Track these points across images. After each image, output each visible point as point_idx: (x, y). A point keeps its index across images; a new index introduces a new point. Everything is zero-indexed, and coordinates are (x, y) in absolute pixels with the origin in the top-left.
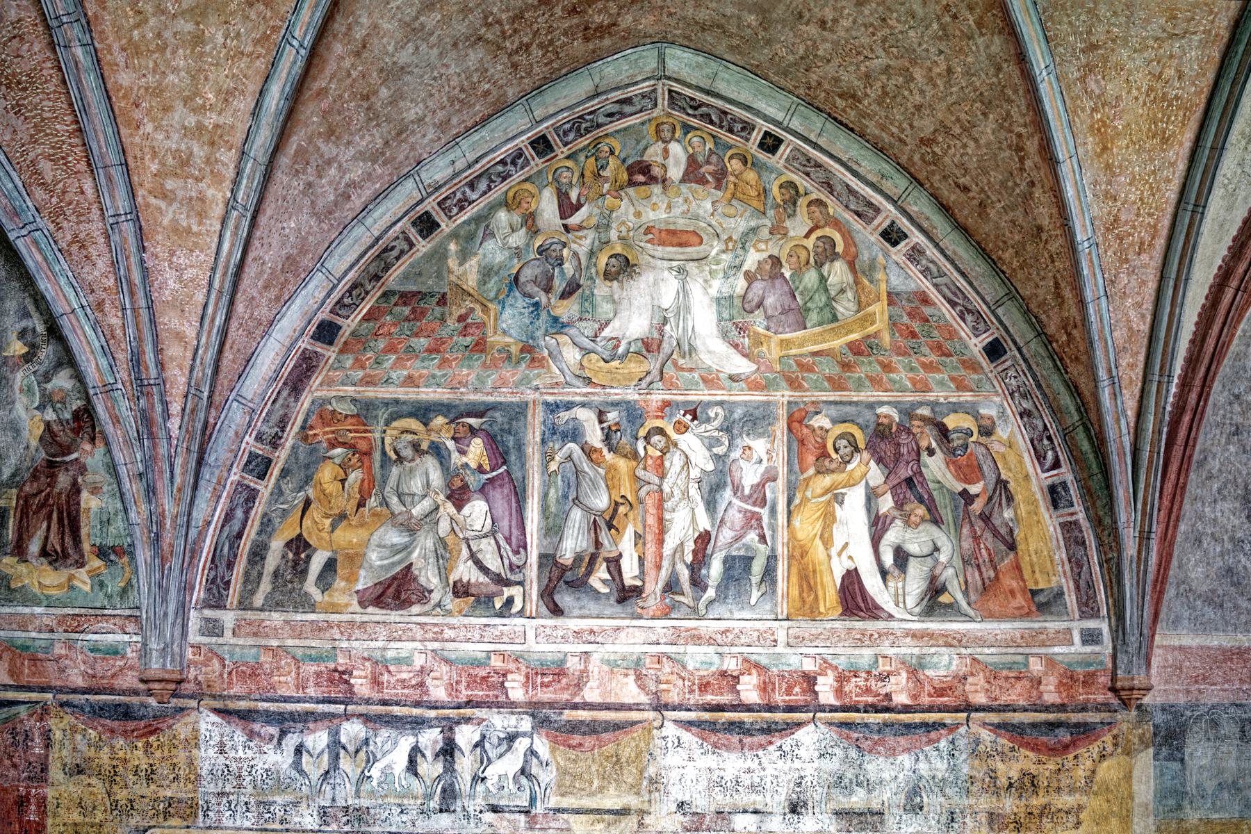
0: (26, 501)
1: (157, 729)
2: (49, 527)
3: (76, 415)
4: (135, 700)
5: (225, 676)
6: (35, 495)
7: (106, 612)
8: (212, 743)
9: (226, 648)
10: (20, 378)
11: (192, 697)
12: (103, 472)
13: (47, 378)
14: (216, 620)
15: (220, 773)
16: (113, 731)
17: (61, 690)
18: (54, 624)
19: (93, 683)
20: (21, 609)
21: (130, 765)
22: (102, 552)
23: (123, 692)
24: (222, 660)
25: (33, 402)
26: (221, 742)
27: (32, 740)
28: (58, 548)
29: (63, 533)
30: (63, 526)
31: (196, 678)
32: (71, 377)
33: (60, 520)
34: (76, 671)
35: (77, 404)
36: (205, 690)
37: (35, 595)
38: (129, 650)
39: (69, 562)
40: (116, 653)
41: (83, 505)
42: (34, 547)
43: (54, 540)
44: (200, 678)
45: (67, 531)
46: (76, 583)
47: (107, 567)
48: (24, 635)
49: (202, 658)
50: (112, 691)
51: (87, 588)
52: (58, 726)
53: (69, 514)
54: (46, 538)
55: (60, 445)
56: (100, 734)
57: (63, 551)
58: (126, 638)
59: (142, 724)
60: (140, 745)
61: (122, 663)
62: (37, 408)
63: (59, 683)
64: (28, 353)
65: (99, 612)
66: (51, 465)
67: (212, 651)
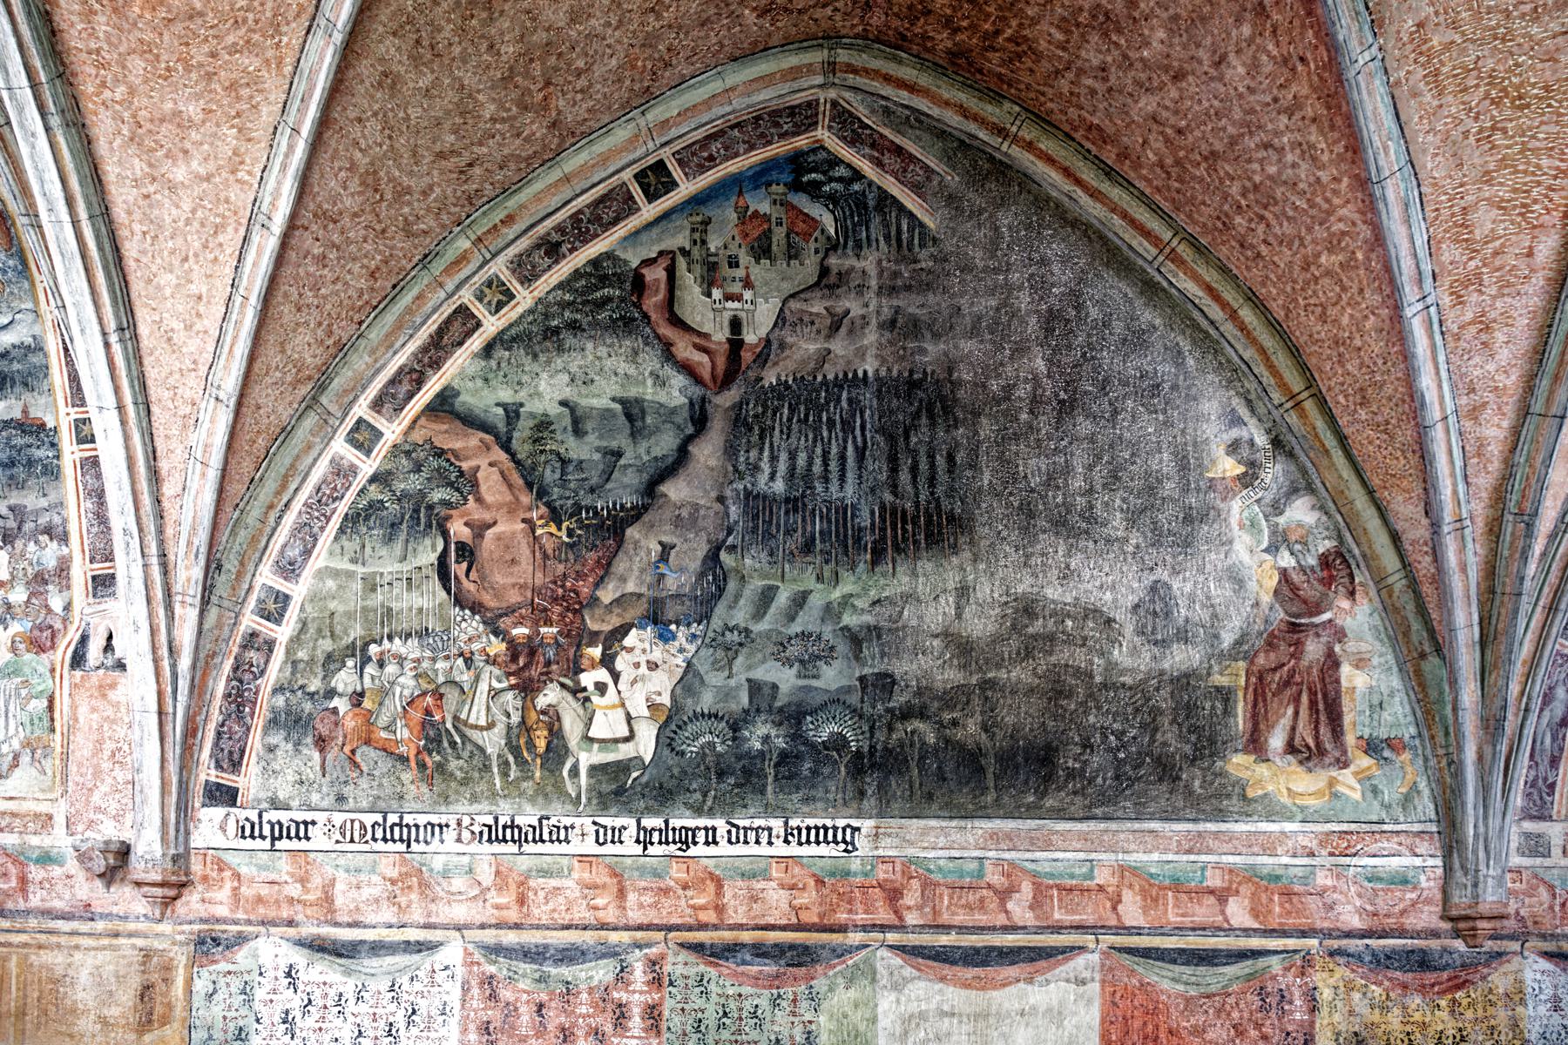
0: (1261, 678)
1: (1466, 981)
2: (1296, 713)
3: (1325, 561)
4: (1434, 944)
5: (1557, 908)
6: (1274, 670)
7: (1385, 827)
8: (1542, 997)
9: (1555, 871)
10: (1237, 508)
11: (1512, 937)
12: (1370, 639)
13: (1277, 508)
14: (1539, 836)
15: (1555, 1036)
16: (1405, 987)
17: (1328, 934)
18: (1314, 845)
19: (1374, 923)
20: (1264, 826)
21: (1431, 1031)
22: (1371, 747)
23: (1417, 935)
24: (1551, 888)
25: (1259, 542)
26: (1555, 996)
27: (1291, 1003)
28: (1312, 744)
29: (1317, 723)
30: (1317, 711)
31: (1517, 913)
32: (1313, 507)
33: (1313, 704)
34: (1349, 908)
35: (1325, 545)
36: (1531, 928)
37: (1285, 807)
38: (1423, 878)
39: (1327, 760)
40: (1405, 882)
41: (1344, 683)
42: (1277, 741)
43: (1305, 733)
44: (1522, 913)
45: (1323, 718)
46: (1340, 788)
47: (1380, 767)
48: (1270, 860)
49: (1524, 886)
50: (1402, 933)
51: (1357, 796)
52: (1326, 983)
53: (1325, 696)
54: (1293, 729)
55: (1305, 602)
56: (1387, 991)
57: (1318, 744)
58: (1418, 862)
59: (1445, 975)
60: (1443, 1003)
61: (1414, 896)
62: (1266, 551)
63: (1326, 925)
64: (1245, 474)
65: (1376, 828)
66: (1294, 628)
67: (1536, 876)
